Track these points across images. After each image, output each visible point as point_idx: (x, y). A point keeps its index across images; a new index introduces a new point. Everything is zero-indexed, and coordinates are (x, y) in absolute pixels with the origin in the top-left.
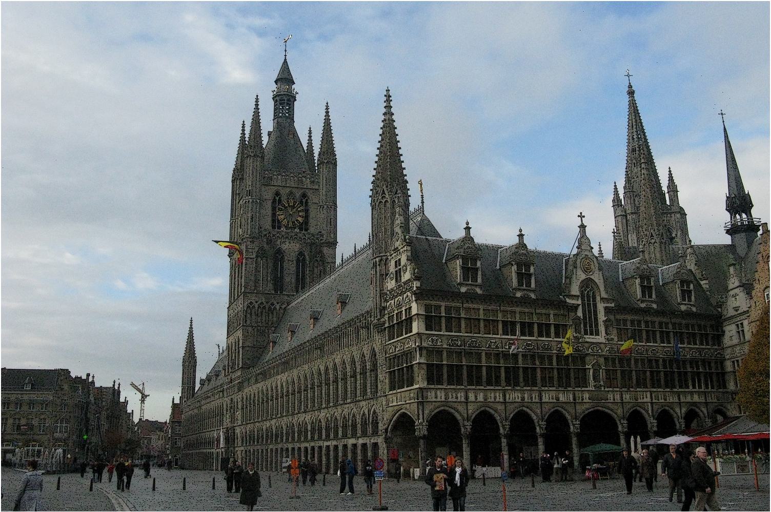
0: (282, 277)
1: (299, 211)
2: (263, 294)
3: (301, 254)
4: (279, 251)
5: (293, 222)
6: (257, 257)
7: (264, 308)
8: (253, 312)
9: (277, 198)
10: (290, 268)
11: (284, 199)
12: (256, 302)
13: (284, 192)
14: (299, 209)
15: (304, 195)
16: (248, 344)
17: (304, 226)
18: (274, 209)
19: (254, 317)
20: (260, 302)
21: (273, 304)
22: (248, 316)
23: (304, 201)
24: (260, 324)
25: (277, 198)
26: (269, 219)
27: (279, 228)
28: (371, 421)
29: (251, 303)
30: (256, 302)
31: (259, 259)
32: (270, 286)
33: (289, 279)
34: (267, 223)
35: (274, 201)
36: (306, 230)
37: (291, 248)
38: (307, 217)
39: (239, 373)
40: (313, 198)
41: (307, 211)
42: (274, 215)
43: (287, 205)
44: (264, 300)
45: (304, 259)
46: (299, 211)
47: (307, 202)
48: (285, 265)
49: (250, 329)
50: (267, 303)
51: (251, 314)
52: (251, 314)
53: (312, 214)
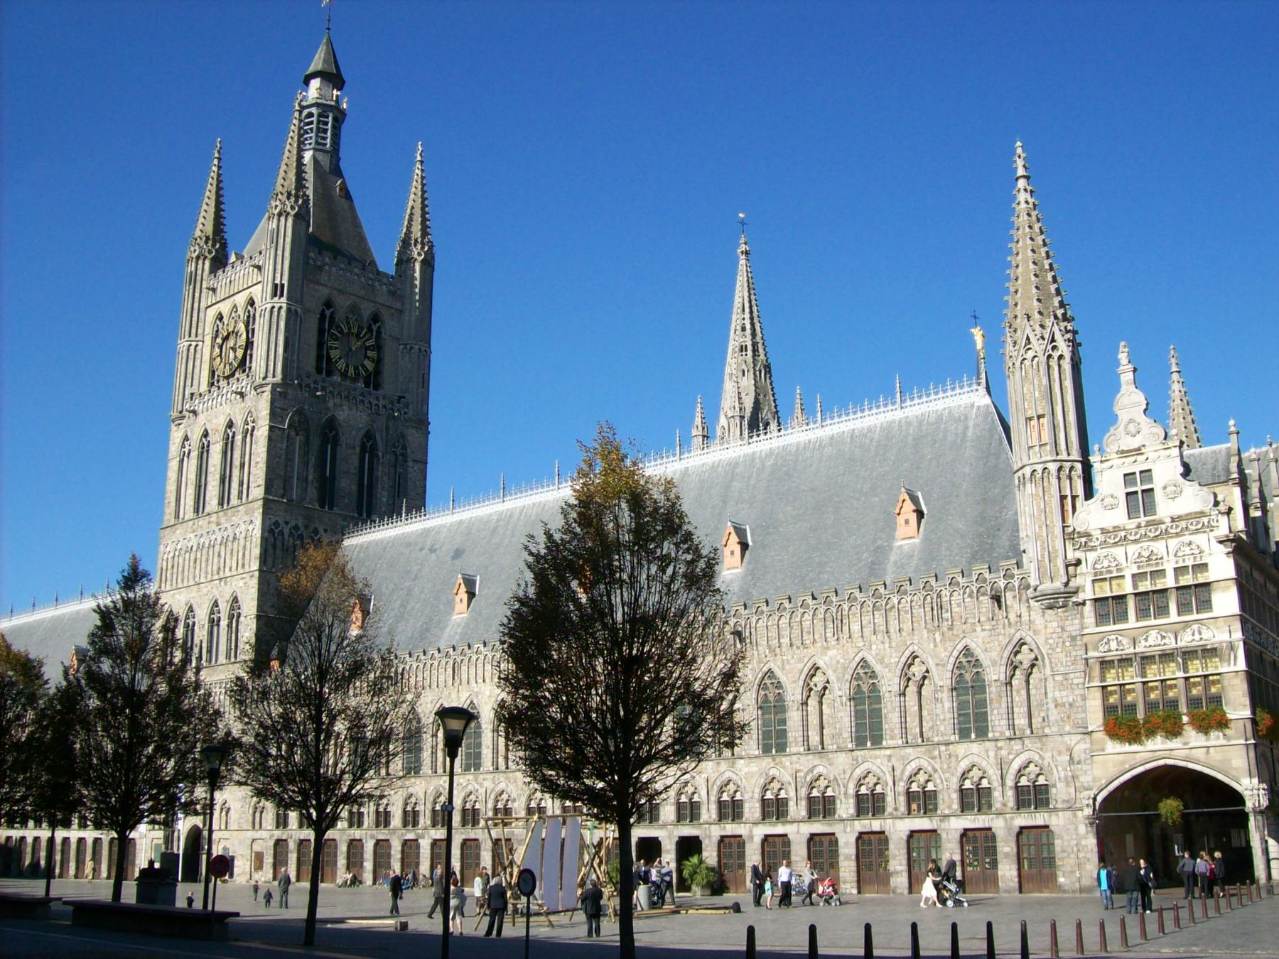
1: (367, 348)
3: (369, 436)
4: (331, 424)
5: (356, 368)
8: (279, 543)
9: (328, 313)
10: (349, 460)
11: (341, 315)
12: (287, 523)
13: (342, 303)
14: (368, 344)
15: (376, 318)
17: (374, 380)
18: (321, 331)
19: (279, 552)
20: (292, 524)
23: (375, 328)
25: (328, 313)
26: (313, 354)
27: (329, 373)
28: (1010, 782)
29: (277, 524)
30: (287, 523)
31: (293, 434)
32: (312, 492)
34: (310, 362)
35: (323, 315)
36: (377, 386)
37: (352, 418)
38: (378, 362)
40: (390, 326)
41: (378, 347)
42: (320, 345)
43: (346, 331)
45: (374, 449)
46: (367, 348)
47: (379, 332)
48: (341, 451)
50: (306, 527)
51: (274, 547)
52: (274, 547)
53: (388, 359)
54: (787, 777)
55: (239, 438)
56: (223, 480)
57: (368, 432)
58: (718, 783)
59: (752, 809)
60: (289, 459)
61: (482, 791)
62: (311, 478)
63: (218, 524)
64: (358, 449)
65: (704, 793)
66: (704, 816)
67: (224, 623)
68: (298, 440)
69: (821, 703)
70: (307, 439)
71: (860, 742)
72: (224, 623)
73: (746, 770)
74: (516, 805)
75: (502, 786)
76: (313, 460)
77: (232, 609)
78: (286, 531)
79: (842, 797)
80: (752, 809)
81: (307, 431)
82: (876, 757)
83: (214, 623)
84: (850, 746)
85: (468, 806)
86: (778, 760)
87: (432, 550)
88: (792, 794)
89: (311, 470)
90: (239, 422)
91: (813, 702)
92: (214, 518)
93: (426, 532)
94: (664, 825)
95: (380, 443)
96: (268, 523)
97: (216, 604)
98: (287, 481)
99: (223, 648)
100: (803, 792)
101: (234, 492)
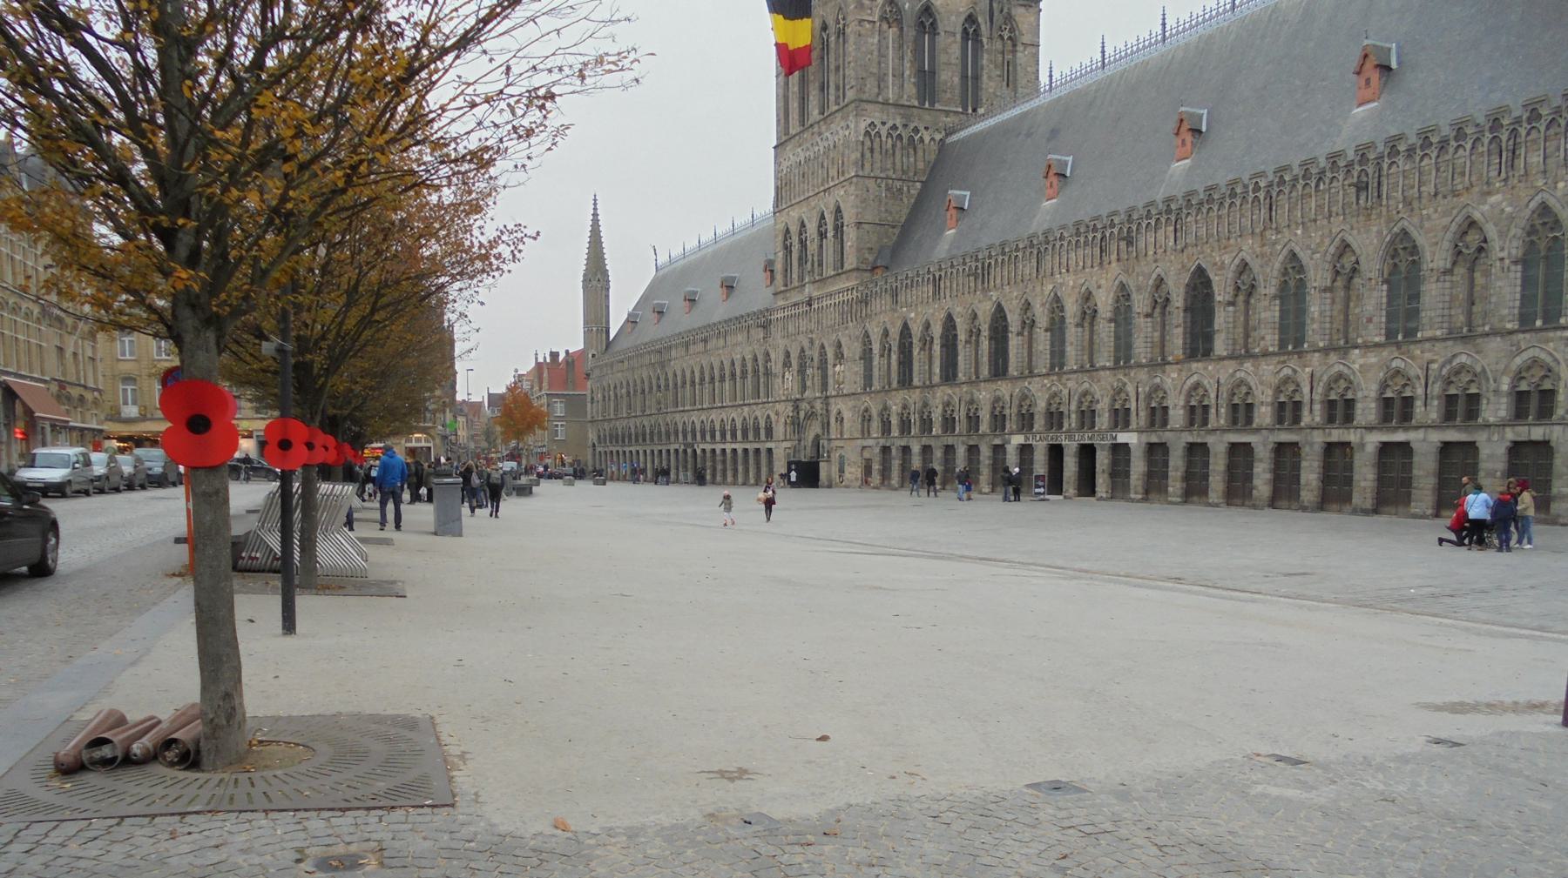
0: (933, 73)
2: (895, 105)
3: (971, 19)
6: (883, 18)
7: (900, 137)
8: (876, 146)
10: (950, 48)
12: (883, 124)
16: (869, 217)
19: (877, 155)
20: (890, 124)
21: (916, 130)
22: (868, 155)
24: (890, 173)
30: (883, 124)
31: (885, 26)
32: (910, 89)
33: (949, 77)
39: (842, 284)
44: (898, 122)
48: (941, 40)
49: (871, 183)
50: (905, 126)
51: (872, 150)
52: (872, 150)
54: (1415, 370)
55: (833, 39)
56: (822, 89)
57: (970, 16)
58: (1325, 378)
59: (1367, 410)
60: (882, 55)
61: (1065, 392)
62: (907, 73)
63: (820, 134)
64: (959, 37)
65: (1306, 390)
66: (1306, 419)
67: (830, 234)
68: (892, 33)
69: (1472, 270)
70: (901, 29)
71: (1526, 322)
72: (830, 234)
73: (1362, 361)
74: (1099, 406)
75: (1086, 385)
76: (909, 56)
77: (836, 219)
78: (884, 133)
79: (1491, 395)
80: (1367, 410)
81: (899, 22)
82: (1547, 341)
83: (822, 235)
84: (1509, 326)
85: (1053, 409)
86: (1404, 348)
87: (1029, 135)
88: (1420, 391)
89: (907, 65)
90: (831, 22)
91: (1461, 271)
92: (816, 129)
93: (1024, 115)
94: (1258, 430)
95: (983, 27)
96: (863, 125)
97: (823, 217)
98: (881, 80)
99: (831, 260)
100: (1436, 389)
101: (832, 98)
